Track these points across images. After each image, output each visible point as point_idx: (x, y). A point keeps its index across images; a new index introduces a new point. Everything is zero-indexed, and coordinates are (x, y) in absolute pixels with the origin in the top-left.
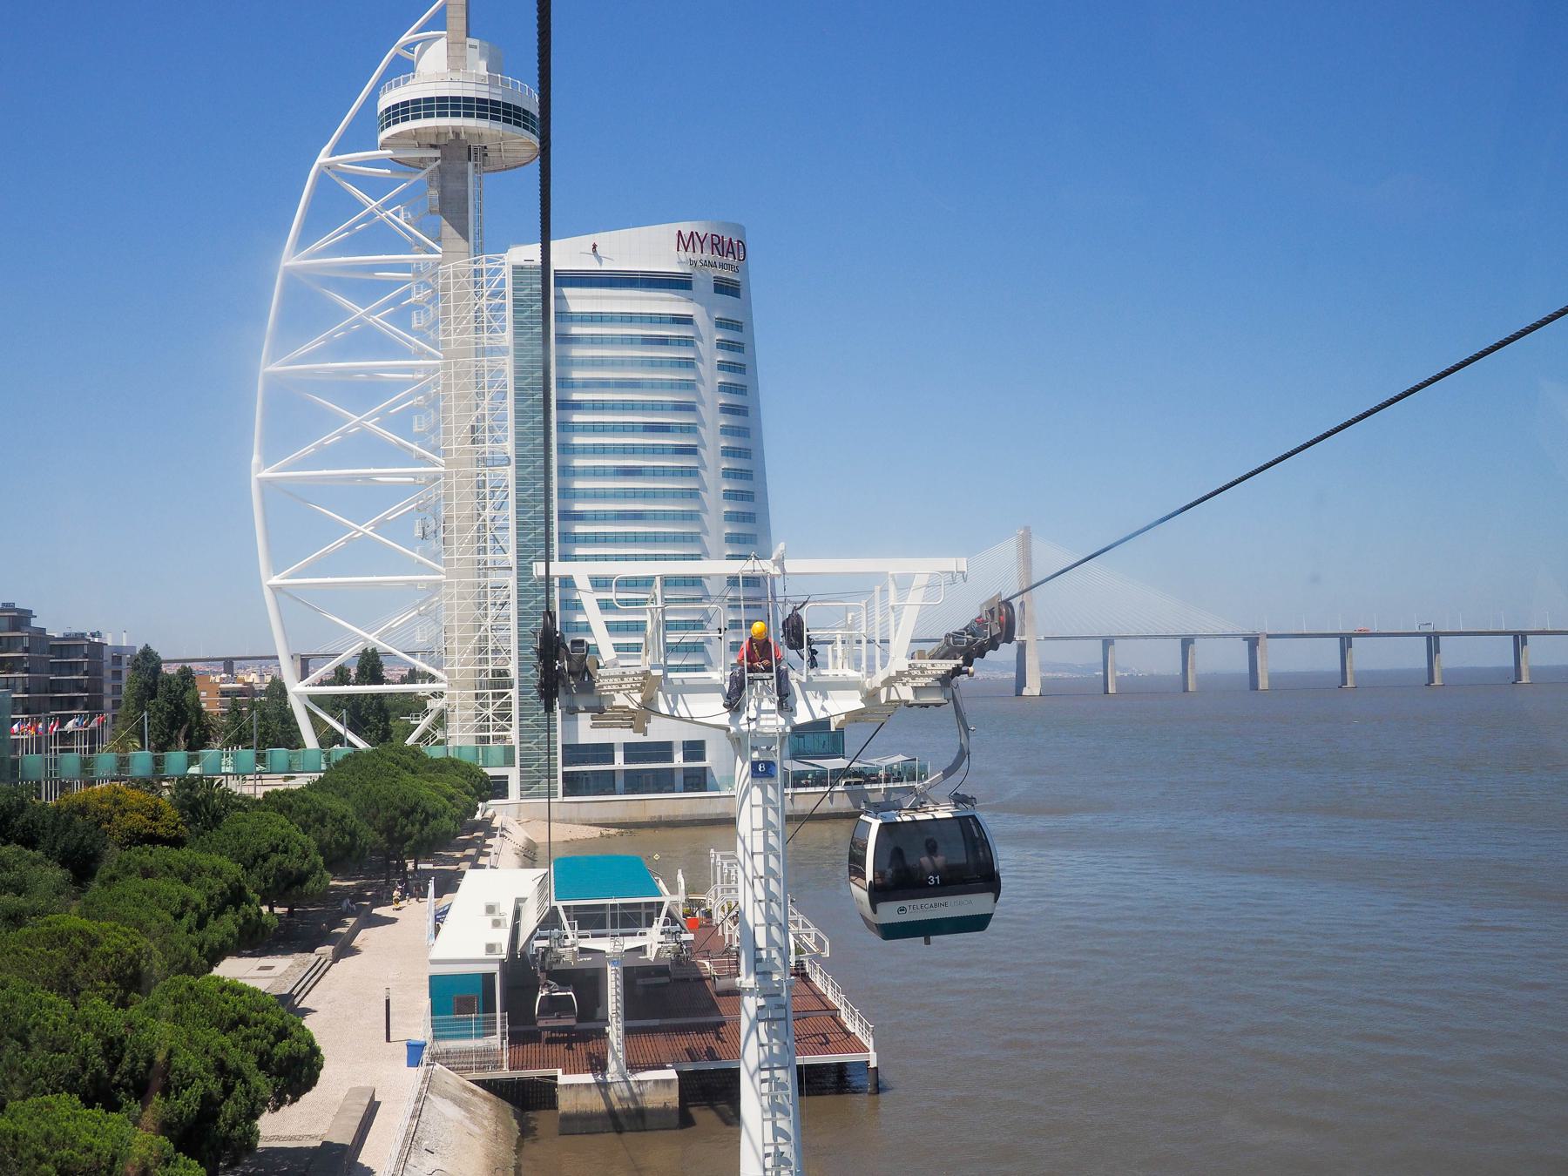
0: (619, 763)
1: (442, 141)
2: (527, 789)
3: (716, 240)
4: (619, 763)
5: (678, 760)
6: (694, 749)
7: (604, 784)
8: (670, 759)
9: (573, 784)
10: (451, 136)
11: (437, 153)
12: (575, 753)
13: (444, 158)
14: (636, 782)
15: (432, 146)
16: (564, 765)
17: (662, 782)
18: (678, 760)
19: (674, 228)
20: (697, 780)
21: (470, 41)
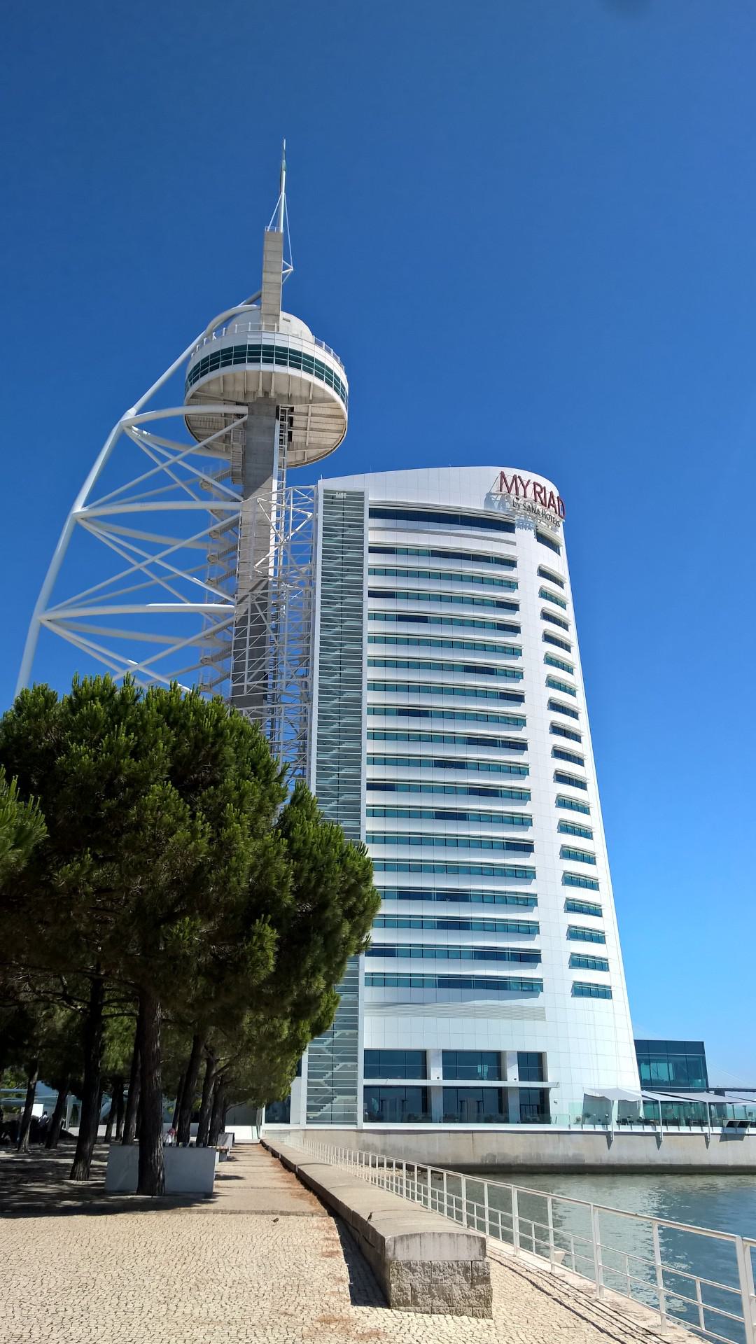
0: (436, 1077)
1: (250, 400)
3: (538, 489)
4: (436, 1077)
5: (512, 1078)
6: (533, 1064)
7: (418, 1106)
9: (381, 1107)
10: (261, 394)
11: (243, 410)
12: (379, 1061)
13: (251, 413)
14: (460, 1107)
15: (238, 404)
17: (494, 1107)
18: (512, 1078)
19: (496, 471)
20: (537, 1107)
21: (283, 315)
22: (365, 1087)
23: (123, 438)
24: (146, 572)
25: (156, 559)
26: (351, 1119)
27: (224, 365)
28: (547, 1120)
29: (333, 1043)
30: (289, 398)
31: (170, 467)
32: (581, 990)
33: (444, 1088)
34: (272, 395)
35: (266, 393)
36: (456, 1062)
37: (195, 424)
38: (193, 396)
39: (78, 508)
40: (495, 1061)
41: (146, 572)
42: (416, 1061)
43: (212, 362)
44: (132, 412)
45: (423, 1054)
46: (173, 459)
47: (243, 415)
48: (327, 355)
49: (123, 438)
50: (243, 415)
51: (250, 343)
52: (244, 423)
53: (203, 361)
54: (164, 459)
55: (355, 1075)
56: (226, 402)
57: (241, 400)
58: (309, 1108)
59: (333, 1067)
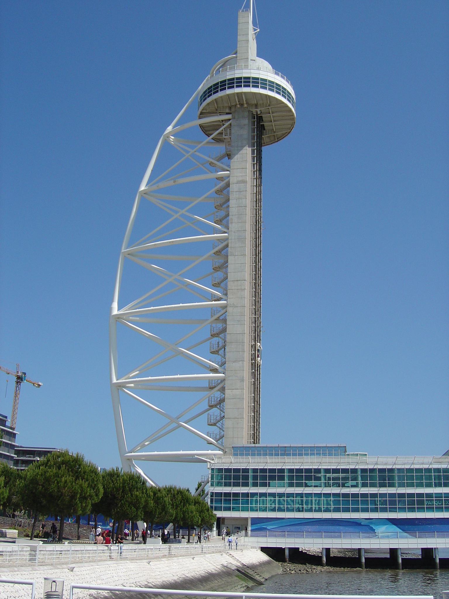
13: (234, 118)
15: (227, 114)
23: (166, 143)
24: (181, 219)
25: (183, 211)
27: (214, 93)
31: (190, 156)
37: (206, 129)
38: (201, 113)
39: (143, 187)
41: (181, 219)
43: (209, 93)
44: (170, 128)
46: (192, 151)
47: (230, 120)
48: (276, 77)
49: (166, 143)
50: (230, 120)
51: (228, 78)
52: (231, 124)
53: (204, 93)
54: (188, 152)
56: (221, 114)
57: (227, 111)
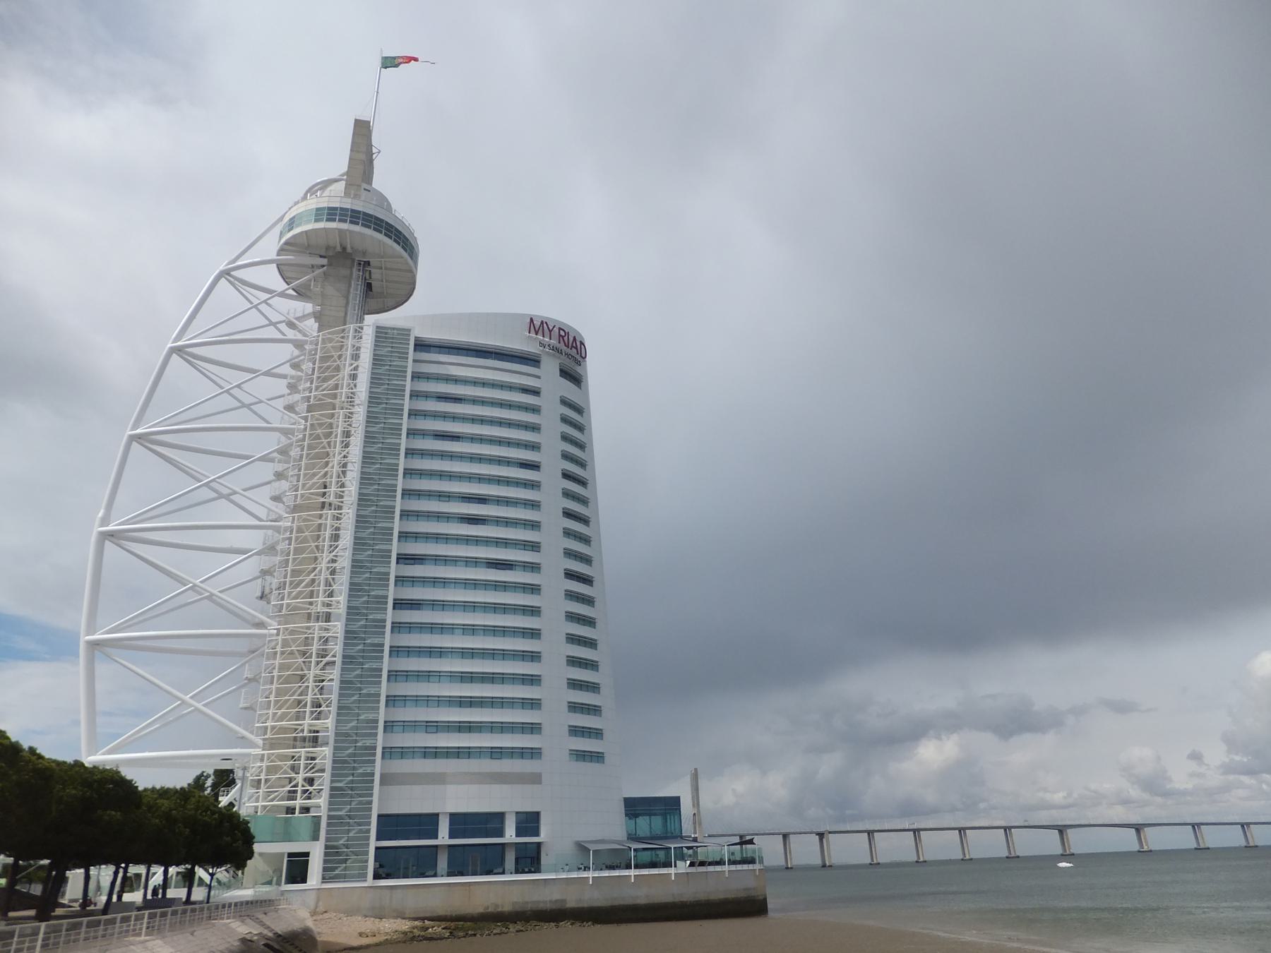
0: (444, 838)
2: (329, 873)
4: (444, 838)
5: (510, 835)
6: (529, 823)
7: (423, 863)
8: (500, 833)
9: (388, 866)
10: (339, 249)
11: (325, 261)
12: (391, 825)
13: (330, 264)
14: (461, 862)
16: (378, 839)
17: (490, 861)
18: (510, 835)
20: (530, 859)
22: (377, 848)
26: (363, 877)
28: (538, 871)
29: (350, 811)
30: (364, 253)
32: (581, 756)
33: (450, 846)
34: (349, 250)
35: (344, 249)
36: (462, 823)
40: (492, 822)
42: (425, 824)
45: (433, 818)
55: (368, 838)
58: (325, 869)
59: (349, 831)
